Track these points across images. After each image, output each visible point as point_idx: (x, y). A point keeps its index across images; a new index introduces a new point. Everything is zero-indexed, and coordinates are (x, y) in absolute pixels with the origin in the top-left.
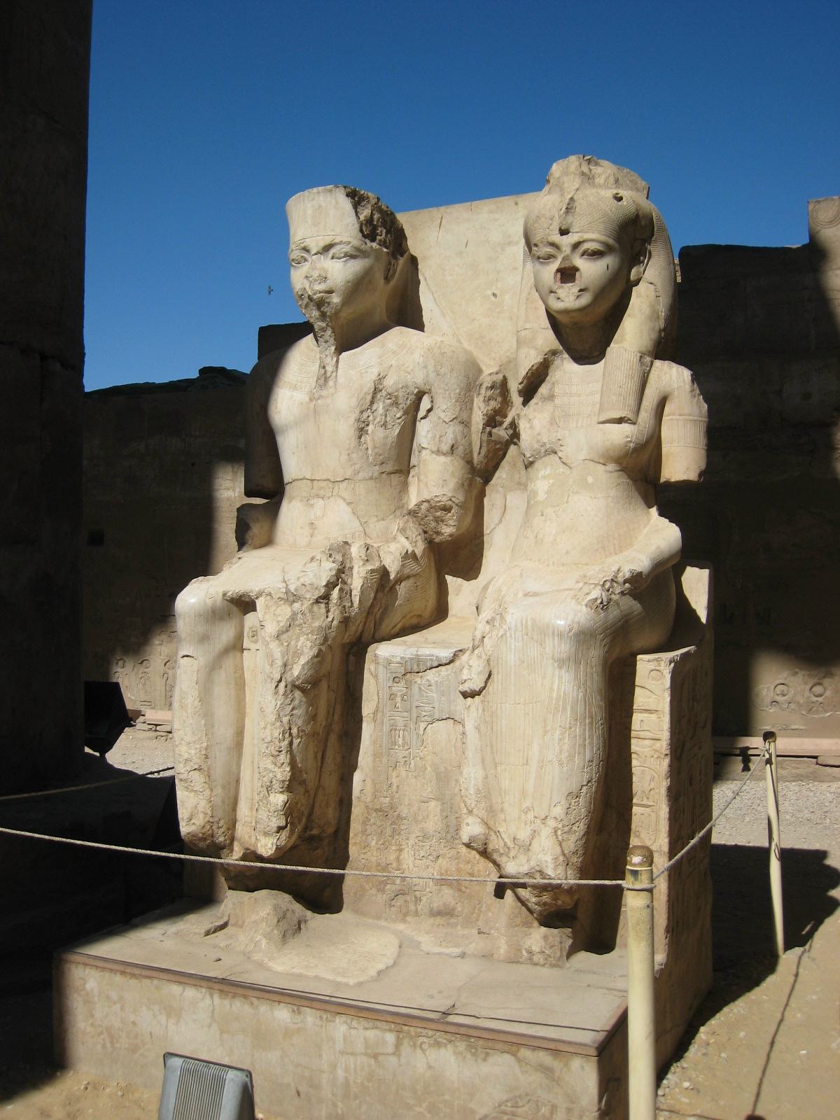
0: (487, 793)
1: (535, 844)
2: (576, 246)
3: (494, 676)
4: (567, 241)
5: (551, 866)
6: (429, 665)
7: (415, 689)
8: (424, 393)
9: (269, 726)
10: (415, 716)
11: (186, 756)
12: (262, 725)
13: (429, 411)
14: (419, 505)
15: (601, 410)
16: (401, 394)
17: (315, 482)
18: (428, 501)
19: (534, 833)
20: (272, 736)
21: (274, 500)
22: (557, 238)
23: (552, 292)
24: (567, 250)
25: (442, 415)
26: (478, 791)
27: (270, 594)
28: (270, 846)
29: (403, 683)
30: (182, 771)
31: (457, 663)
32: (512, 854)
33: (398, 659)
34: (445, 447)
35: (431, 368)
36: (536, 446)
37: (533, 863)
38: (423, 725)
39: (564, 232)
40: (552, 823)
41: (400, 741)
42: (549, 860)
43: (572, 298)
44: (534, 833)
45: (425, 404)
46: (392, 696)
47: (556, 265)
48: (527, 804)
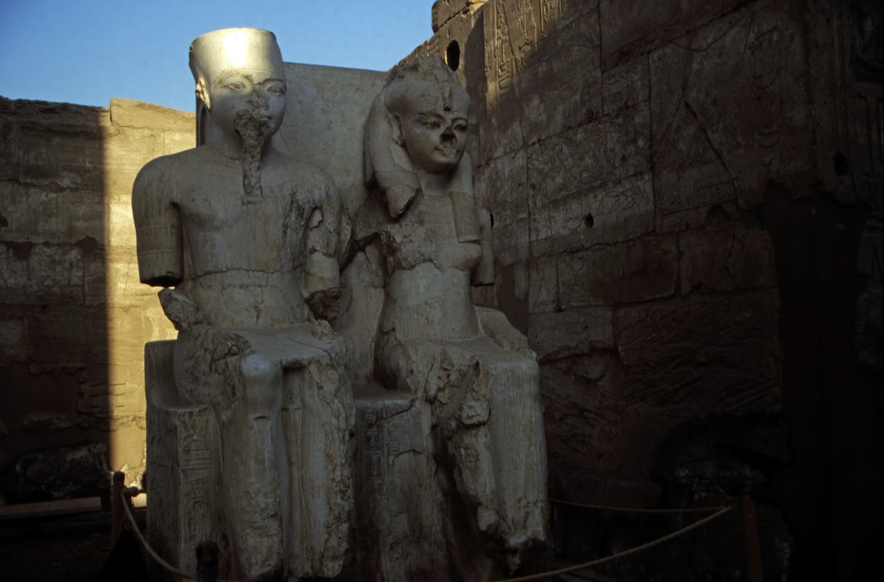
0: (498, 492)
1: (531, 521)
2: (454, 120)
3: (494, 412)
4: (449, 117)
5: (542, 533)
6: (394, 412)
7: (386, 430)
8: (316, 208)
9: (338, 468)
10: (386, 451)
11: (263, 505)
12: (330, 468)
13: (320, 222)
14: (313, 295)
15: (459, 234)
16: (307, 207)
17: (251, 273)
18: (324, 292)
19: (527, 515)
20: (342, 476)
21: (181, 286)
22: (441, 112)
23: (436, 149)
24: (449, 122)
25: (329, 227)
26: (492, 492)
27: (318, 362)
28: (337, 567)
29: (375, 428)
30: (258, 519)
31: (414, 409)
32: (513, 531)
33: (371, 410)
34: (331, 251)
35: (323, 190)
36: (418, 255)
37: (529, 534)
38: (391, 459)
39: (447, 109)
40: (540, 505)
41: (375, 473)
42: (541, 528)
43: (453, 156)
44: (527, 515)
45: (317, 217)
46: (368, 439)
47: (442, 130)
48: (520, 494)
